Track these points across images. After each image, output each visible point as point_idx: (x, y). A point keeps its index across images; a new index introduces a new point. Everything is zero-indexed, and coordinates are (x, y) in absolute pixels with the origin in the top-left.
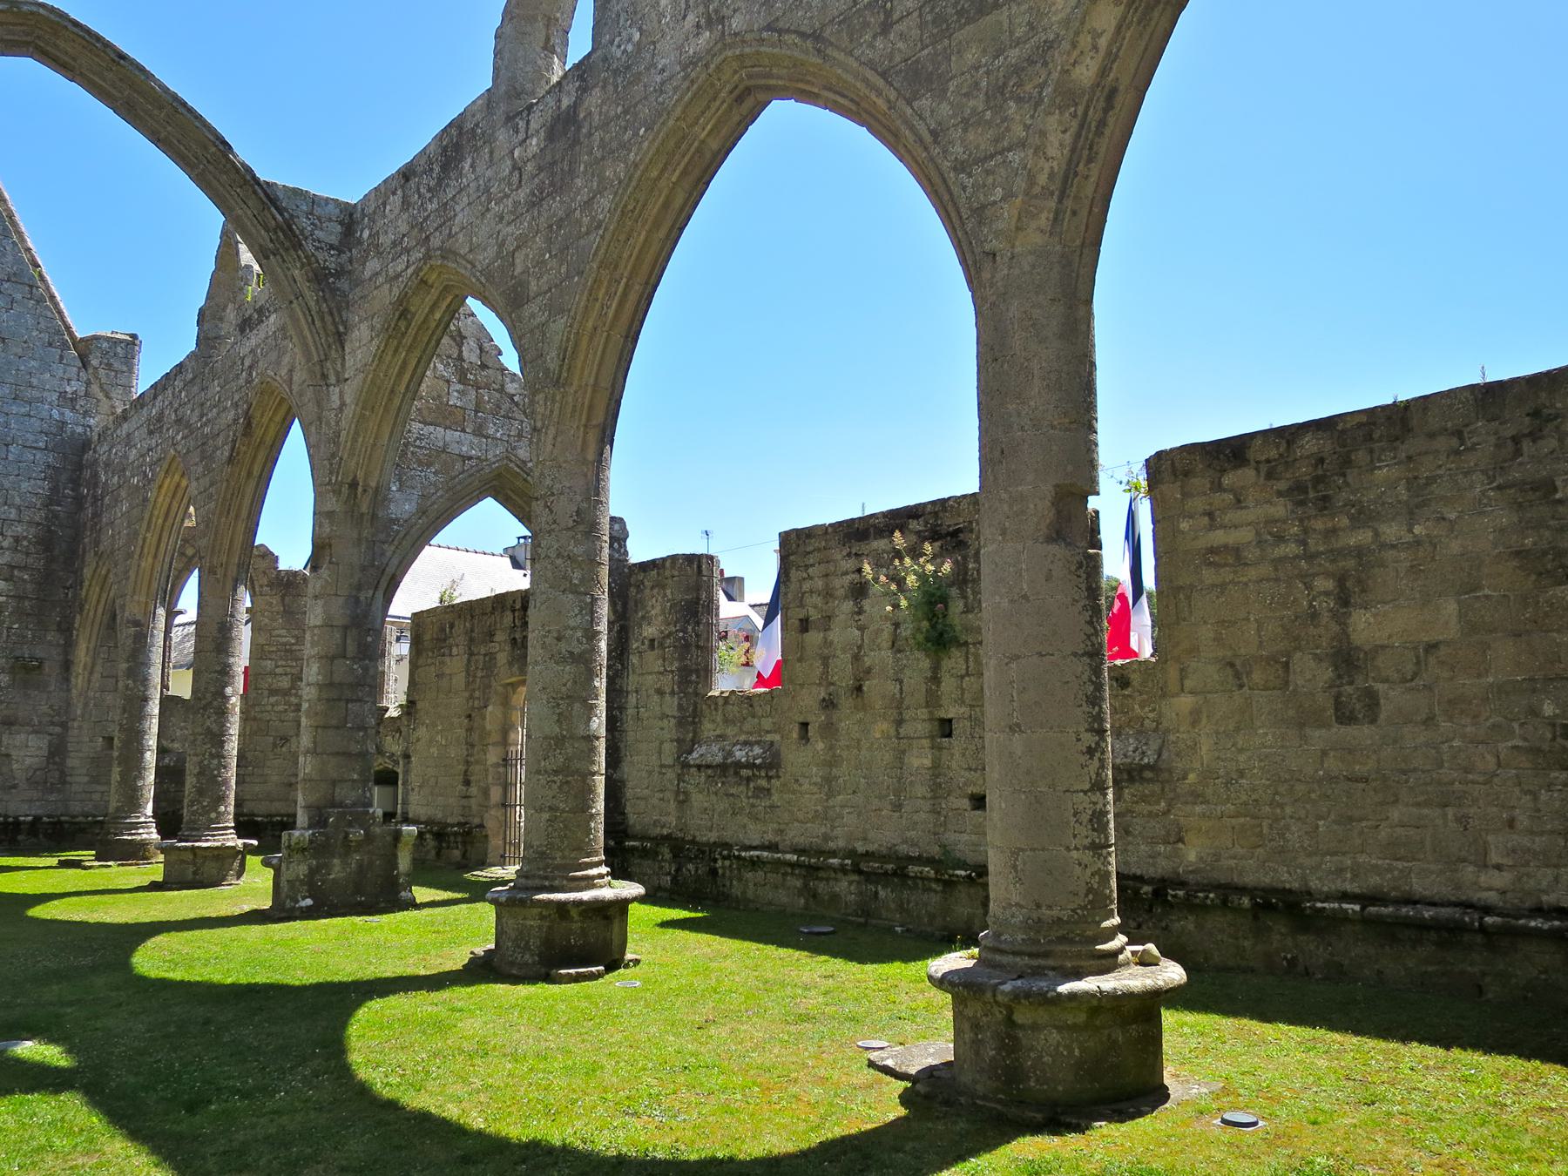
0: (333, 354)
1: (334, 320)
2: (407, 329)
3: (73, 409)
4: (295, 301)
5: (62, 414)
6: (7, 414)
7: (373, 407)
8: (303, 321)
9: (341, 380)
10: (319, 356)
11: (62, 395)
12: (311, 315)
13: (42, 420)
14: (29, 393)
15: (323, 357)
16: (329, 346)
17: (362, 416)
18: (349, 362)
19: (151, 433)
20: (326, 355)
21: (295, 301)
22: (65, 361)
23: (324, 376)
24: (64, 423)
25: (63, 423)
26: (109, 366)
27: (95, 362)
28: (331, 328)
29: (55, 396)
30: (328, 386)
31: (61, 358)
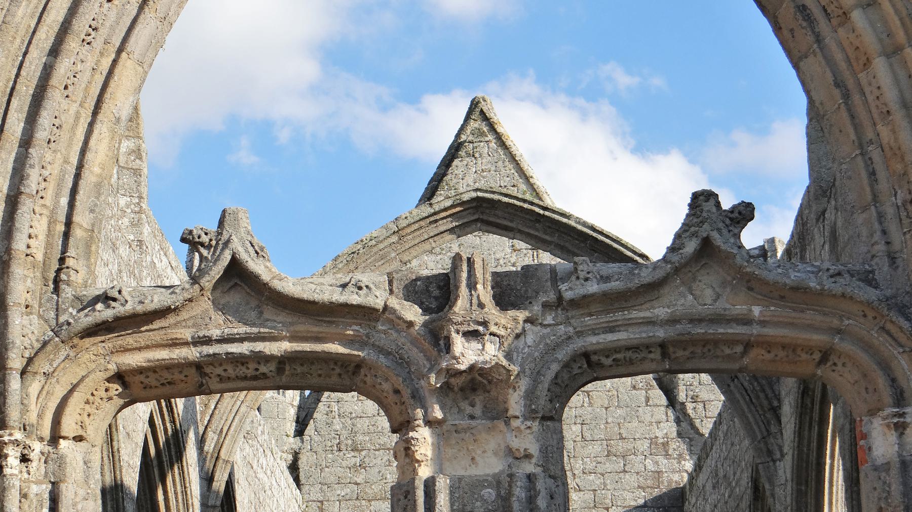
0: (773, 429)
1: (766, 396)
2: (813, 404)
3: (667, 455)
4: (732, 384)
5: (657, 463)
6: (603, 475)
7: (807, 481)
8: (742, 402)
9: (783, 455)
10: (762, 434)
11: (653, 441)
12: (749, 395)
13: (638, 473)
14: (621, 446)
15: (765, 434)
16: (769, 423)
17: (799, 491)
18: (785, 437)
19: (714, 488)
20: (768, 431)
21: (732, 384)
22: (651, 402)
23: (770, 453)
24: (659, 473)
25: (658, 472)
26: (695, 399)
27: (682, 396)
28: (765, 403)
29: (646, 444)
30: (774, 461)
31: (647, 399)
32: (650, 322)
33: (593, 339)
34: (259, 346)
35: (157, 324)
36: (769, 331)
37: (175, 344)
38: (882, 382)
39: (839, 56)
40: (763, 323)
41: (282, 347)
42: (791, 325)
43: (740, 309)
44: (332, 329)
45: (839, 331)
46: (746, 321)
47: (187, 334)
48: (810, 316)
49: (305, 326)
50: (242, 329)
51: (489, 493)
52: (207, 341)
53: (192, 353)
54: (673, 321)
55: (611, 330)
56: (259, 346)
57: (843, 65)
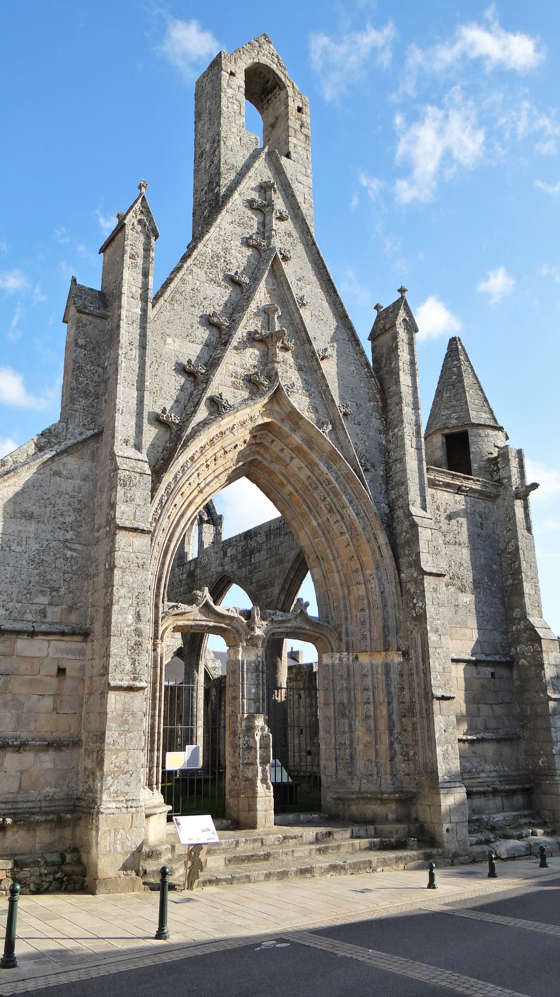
32: (287, 627)
33: (277, 630)
34: (208, 623)
35: (187, 615)
36: (310, 632)
37: (189, 620)
38: (329, 647)
39: (324, 569)
40: (308, 630)
41: (211, 624)
42: (313, 631)
43: (304, 626)
44: (224, 621)
45: (321, 634)
46: (305, 629)
47: (192, 618)
48: (317, 630)
49: (217, 620)
50: (205, 618)
51: (253, 665)
52: (196, 620)
53: (192, 623)
54: (291, 627)
55: (279, 628)
56: (208, 623)
57: (325, 572)
